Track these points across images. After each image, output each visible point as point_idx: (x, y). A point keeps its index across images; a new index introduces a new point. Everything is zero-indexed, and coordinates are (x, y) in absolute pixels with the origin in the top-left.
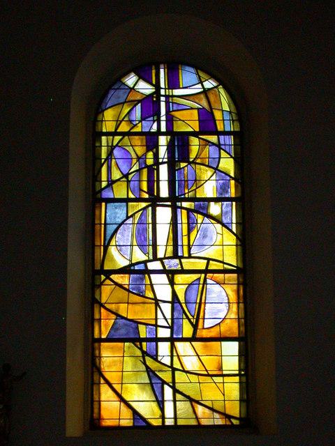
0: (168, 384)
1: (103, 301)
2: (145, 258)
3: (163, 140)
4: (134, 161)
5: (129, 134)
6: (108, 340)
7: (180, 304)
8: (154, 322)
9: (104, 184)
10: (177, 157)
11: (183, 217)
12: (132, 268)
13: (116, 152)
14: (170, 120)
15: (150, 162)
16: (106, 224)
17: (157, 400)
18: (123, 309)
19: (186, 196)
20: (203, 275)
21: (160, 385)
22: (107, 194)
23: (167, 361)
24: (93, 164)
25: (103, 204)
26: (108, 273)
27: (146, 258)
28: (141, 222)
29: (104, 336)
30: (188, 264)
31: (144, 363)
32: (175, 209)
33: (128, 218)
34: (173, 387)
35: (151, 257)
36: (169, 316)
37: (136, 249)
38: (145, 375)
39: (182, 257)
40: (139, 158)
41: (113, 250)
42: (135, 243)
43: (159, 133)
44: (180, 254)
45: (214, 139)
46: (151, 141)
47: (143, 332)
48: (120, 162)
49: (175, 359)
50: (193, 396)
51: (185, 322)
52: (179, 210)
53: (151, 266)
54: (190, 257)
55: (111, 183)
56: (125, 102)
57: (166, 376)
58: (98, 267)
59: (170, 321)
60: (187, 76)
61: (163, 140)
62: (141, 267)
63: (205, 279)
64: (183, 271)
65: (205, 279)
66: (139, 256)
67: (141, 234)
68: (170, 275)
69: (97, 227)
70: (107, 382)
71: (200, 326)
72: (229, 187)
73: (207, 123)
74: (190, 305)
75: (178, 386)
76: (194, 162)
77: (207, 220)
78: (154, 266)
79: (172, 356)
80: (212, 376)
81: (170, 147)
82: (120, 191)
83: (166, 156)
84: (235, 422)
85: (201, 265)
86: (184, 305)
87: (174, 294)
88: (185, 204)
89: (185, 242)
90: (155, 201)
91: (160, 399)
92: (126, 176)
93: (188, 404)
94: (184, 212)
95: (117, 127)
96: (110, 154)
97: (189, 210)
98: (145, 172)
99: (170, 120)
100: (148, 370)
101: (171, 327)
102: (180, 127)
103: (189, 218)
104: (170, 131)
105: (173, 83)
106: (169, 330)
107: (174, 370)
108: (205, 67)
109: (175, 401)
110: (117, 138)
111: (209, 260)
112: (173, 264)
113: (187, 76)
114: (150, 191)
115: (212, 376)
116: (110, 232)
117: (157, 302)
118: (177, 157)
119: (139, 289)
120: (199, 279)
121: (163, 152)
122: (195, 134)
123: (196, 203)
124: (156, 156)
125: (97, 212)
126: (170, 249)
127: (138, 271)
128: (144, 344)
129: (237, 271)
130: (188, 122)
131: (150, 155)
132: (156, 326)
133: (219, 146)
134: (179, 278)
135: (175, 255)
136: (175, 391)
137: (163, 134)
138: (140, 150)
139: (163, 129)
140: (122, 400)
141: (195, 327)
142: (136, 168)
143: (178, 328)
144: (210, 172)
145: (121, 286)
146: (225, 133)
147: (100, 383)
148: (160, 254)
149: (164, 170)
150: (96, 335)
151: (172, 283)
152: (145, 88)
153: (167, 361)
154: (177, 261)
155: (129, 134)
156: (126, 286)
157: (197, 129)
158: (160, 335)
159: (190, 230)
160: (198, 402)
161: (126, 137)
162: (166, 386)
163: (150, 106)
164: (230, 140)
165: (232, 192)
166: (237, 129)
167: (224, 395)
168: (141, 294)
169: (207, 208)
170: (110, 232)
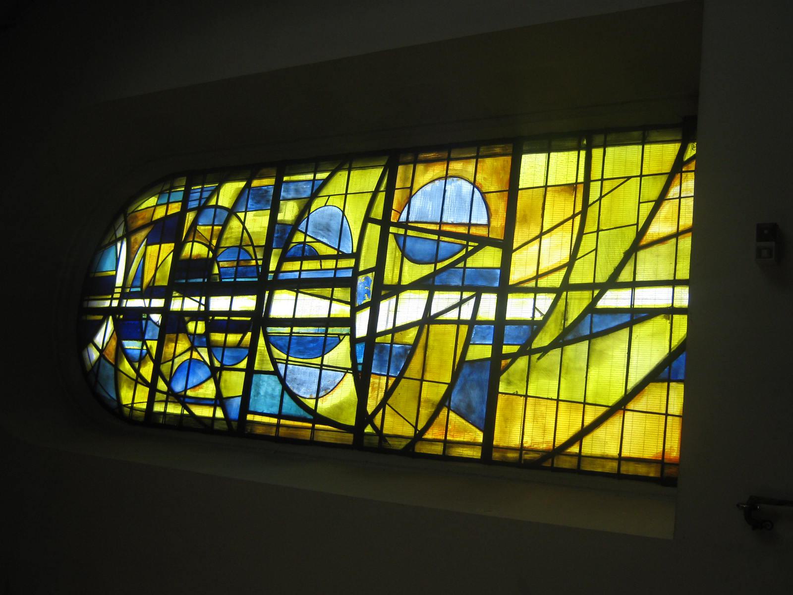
0: (595, 300)
1: (409, 431)
2: (345, 344)
4: (195, 355)
6: (488, 428)
7: (436, 272)
8: (464, 329)
9: (220, 414)
10: (201, 280)
12: (360, 368)
13: (178, 387)
14: (152, 291)
15: (201, 327)
16: (279, 416)
17: (630, 325)
18: (433, 392)
19: (260, 262)
20: (392, 230)
21: (596, 318)
22: (234, 413)
23: (545, 302)
25: (250, 417)
26: (363, 417)
27: (347, 338)
29: (479, 437)
30: (368, 260)
31: (544, 350)
33: (276, 372)
34: (603, 288)
35: (346, 330)
36: (455, 296)
37: (330, 358)
38: (570, 350)
39: (355, 269)
40: (192, 348)
41: (325, 406)
42: (317, 361)
43: (164, 311)
44: (349, 274)
47: (481, 351)
48: (193, 381)
49: (543, 283)
50: (627, 246)
51: (471, 262)
52: (282, 276)
53: (361, 331)
54: (356, 256)
55: (219, 400)
57: (578, 303)
58: (349, 438)
59: (466, 295)
61: (176, 305)
62: (360, 348)
63: (399, 225)
64: (379, 268)
65: (399, 225)
66: (340, 355)
68: (383, 293)
69: (282, 431)
70: (578, 438)
71: (482, 232)
72: (259, 188)
74: (442, 253)
75: (602, 278)
77: (303, 226)
78: (361, 331)
79: (537, 290)
80: (586, 205)
81: (187, 292)
82: (234, 382)
83: (198, 299)
84: (691, 152)
85: (374, 231)
86: (440, 266)
88: (273, 266)
89: (330, 264)
91: (626, 318)
92: (213, 369)
93: (641, 254)
94: (288, 266)
95: (145, 383)
96: (182, 399)
97: (282, 260)
98: (218, 337)
100: (560, 343)
101: (478, 292)
103: (293, 259)
104: (166, 293)
106: (484, 296)
107: (566, 286)
109: (634, 285)
111: (368, 219)
114: (239, 328)
115: (586, 205)
117: (429, 320)
118: (201, 280)
119: (400, 356)
120: (396, 236)
121: (191, 305)
123: (274, 245)
124: (195, 316)
125: (260, 430)
126: (339, 293)
128: (506, 349)
133: (200, 210)
134: (390, 277)
135: (350, 283)
136: (613, 283)
137: (168, 303)
138: (183, 345)
140: (620, 406)
141: (484, 242)
142: (204, 353)
143: (481, 276)
144: (235, 224)
145: (389, 393)
146: (185, 202)
147: (579, 456)
148: (342, 311)
149: (219, 303)
150: (475, 453)
151: (396, 290)
152: (105, 334)
153: (545, 302)
154: (361, 279)
156: (391, 382)
158: (492, 316)
159: (315, 256)
160: (641, 233)
162: (601, 304)
167: (629, 178)
168: (409, 352)
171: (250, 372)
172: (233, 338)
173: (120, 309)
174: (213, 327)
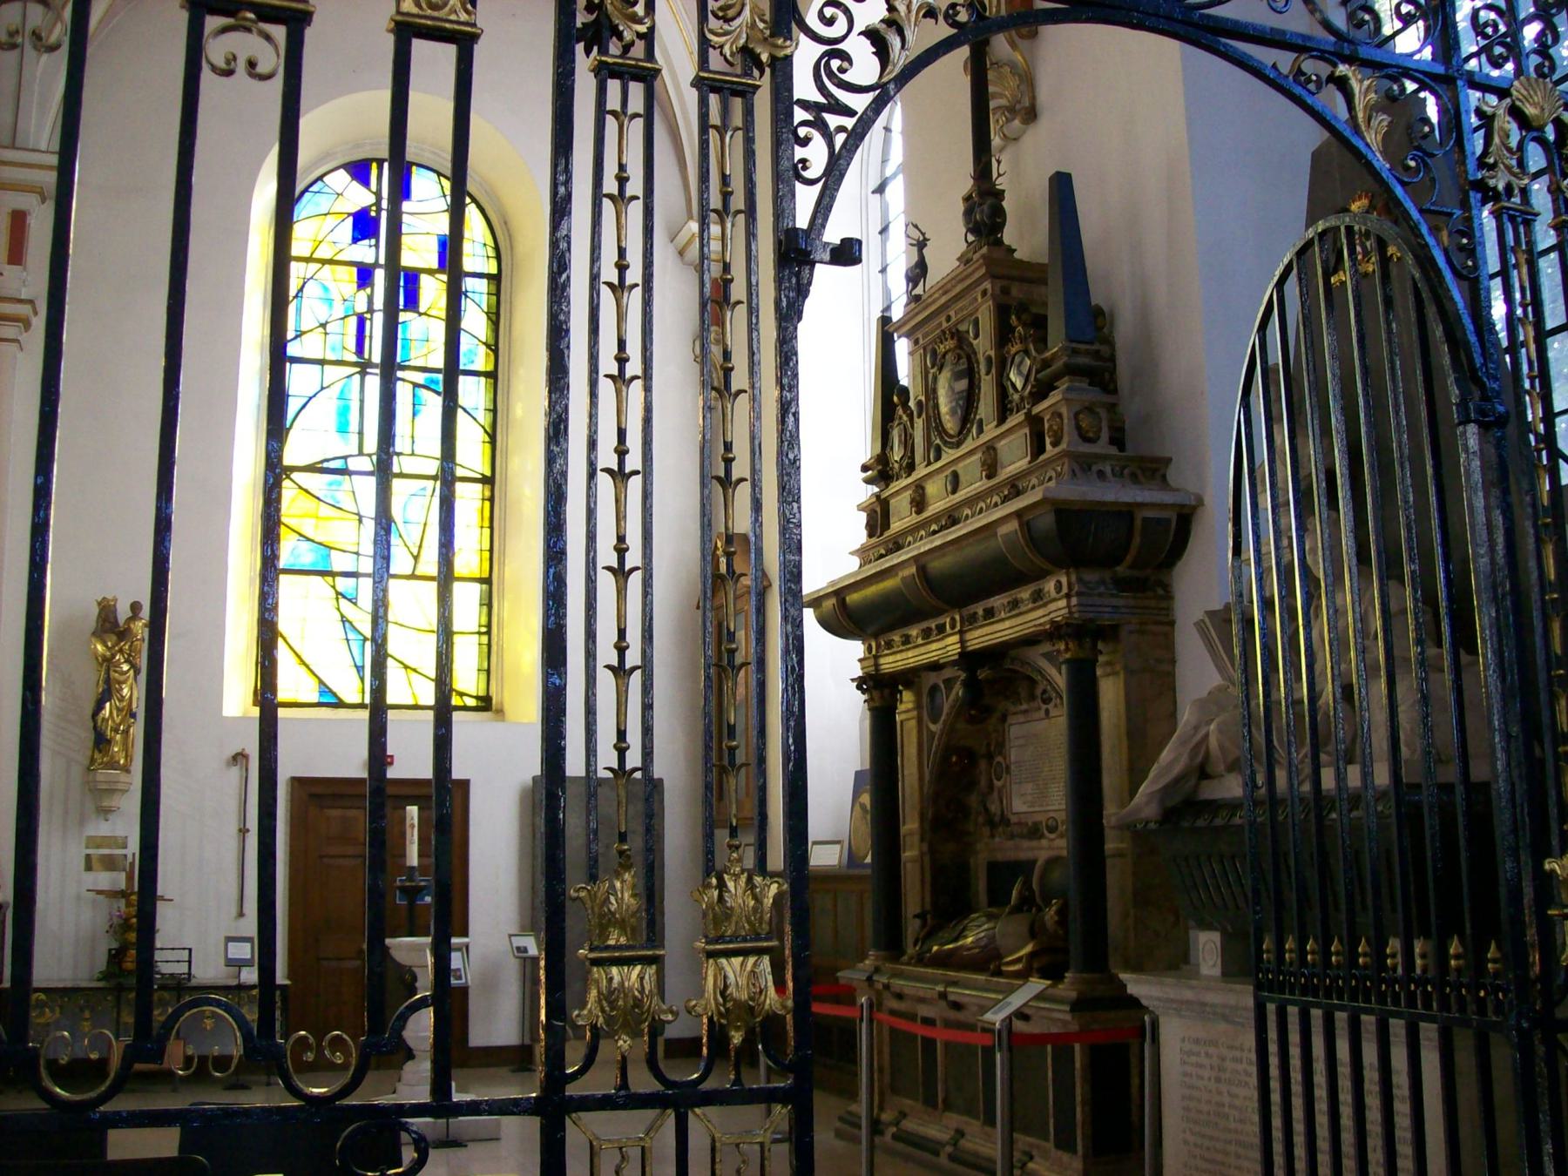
5: (331, 262)
15: (361, 307)
43: (376, 265)
46: (365, 276)
56: (328, 213)
61: (379, 276)
76: (425, 314)
97: (416, 385)
100: (344, 620)
110: (314, 266)
122: (430, 272)
155: (331, 262)
161: (327, 266)
171: (322, 362)
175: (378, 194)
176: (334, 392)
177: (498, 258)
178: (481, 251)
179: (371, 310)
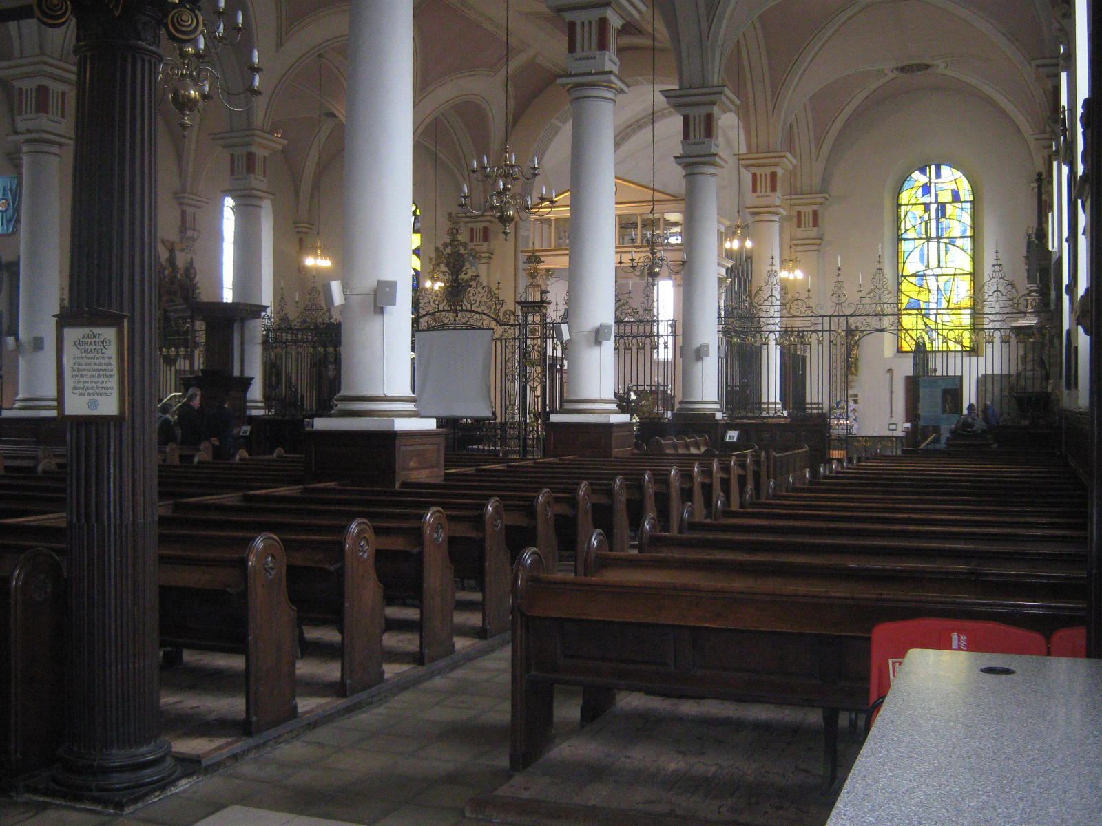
3: (933, 208)
5: (915, 204)
9: (903, 231)
11: (942, 246)
14: (937, 196)
15: (926, 218)
22: (904, 236)
24: (897, 220)
26: (905, 277)
28: (922, 251)
30: (945, 271)
32: (939, 243)
43: (931, 203)
45: (959, 205)
46: (927, 207)
47: (923, 306)
48: (911, 220)
55: (906, 231)
60: (945, 170)
61: (933, 208)
62: (922, 273)
67: (922, 256)
73: (956, 197)
81: (937, 210)
82: (911, 234)
87: (938, 287)
90: (928, 239)
92: (914, 227)
96: (906, 215)
97: (946, 244)
98: (924, 224)
99: (937, 196)
102: (940, 200)
103: (946, 247)
104: (936, 202)
105: (938, 175)
108: (955, 165)
110: (910, 207)
112: (938, 271)
113: (945, 170)
116: (906, 256)
121: (933, 215)
122: (949, 203)
124: (929, 215)
127: (920, 275)
129: (971, 274)
130: (946, 197)
131: (926, 215)
132: (929, 302)
133: (962, 209)
135: (939, 267)
139: (933, 201)
142: (920, 222)
151: (937, 281)
155: (915, 204)
157: (951, 200)
158: (931, 307)
163: (926, 189)
164: (968, 205)
165: (969, 233)
166: (972, 199)
169: (954, 242)
170: (906, 256)
171: (915, 239)
172: (923, 231)
173: (930, 183)
174: (926, 223)
175: (930, 178)
176: (919, 249)
177: (973, 194)
178: (967, 193)
179: (930, 219)
